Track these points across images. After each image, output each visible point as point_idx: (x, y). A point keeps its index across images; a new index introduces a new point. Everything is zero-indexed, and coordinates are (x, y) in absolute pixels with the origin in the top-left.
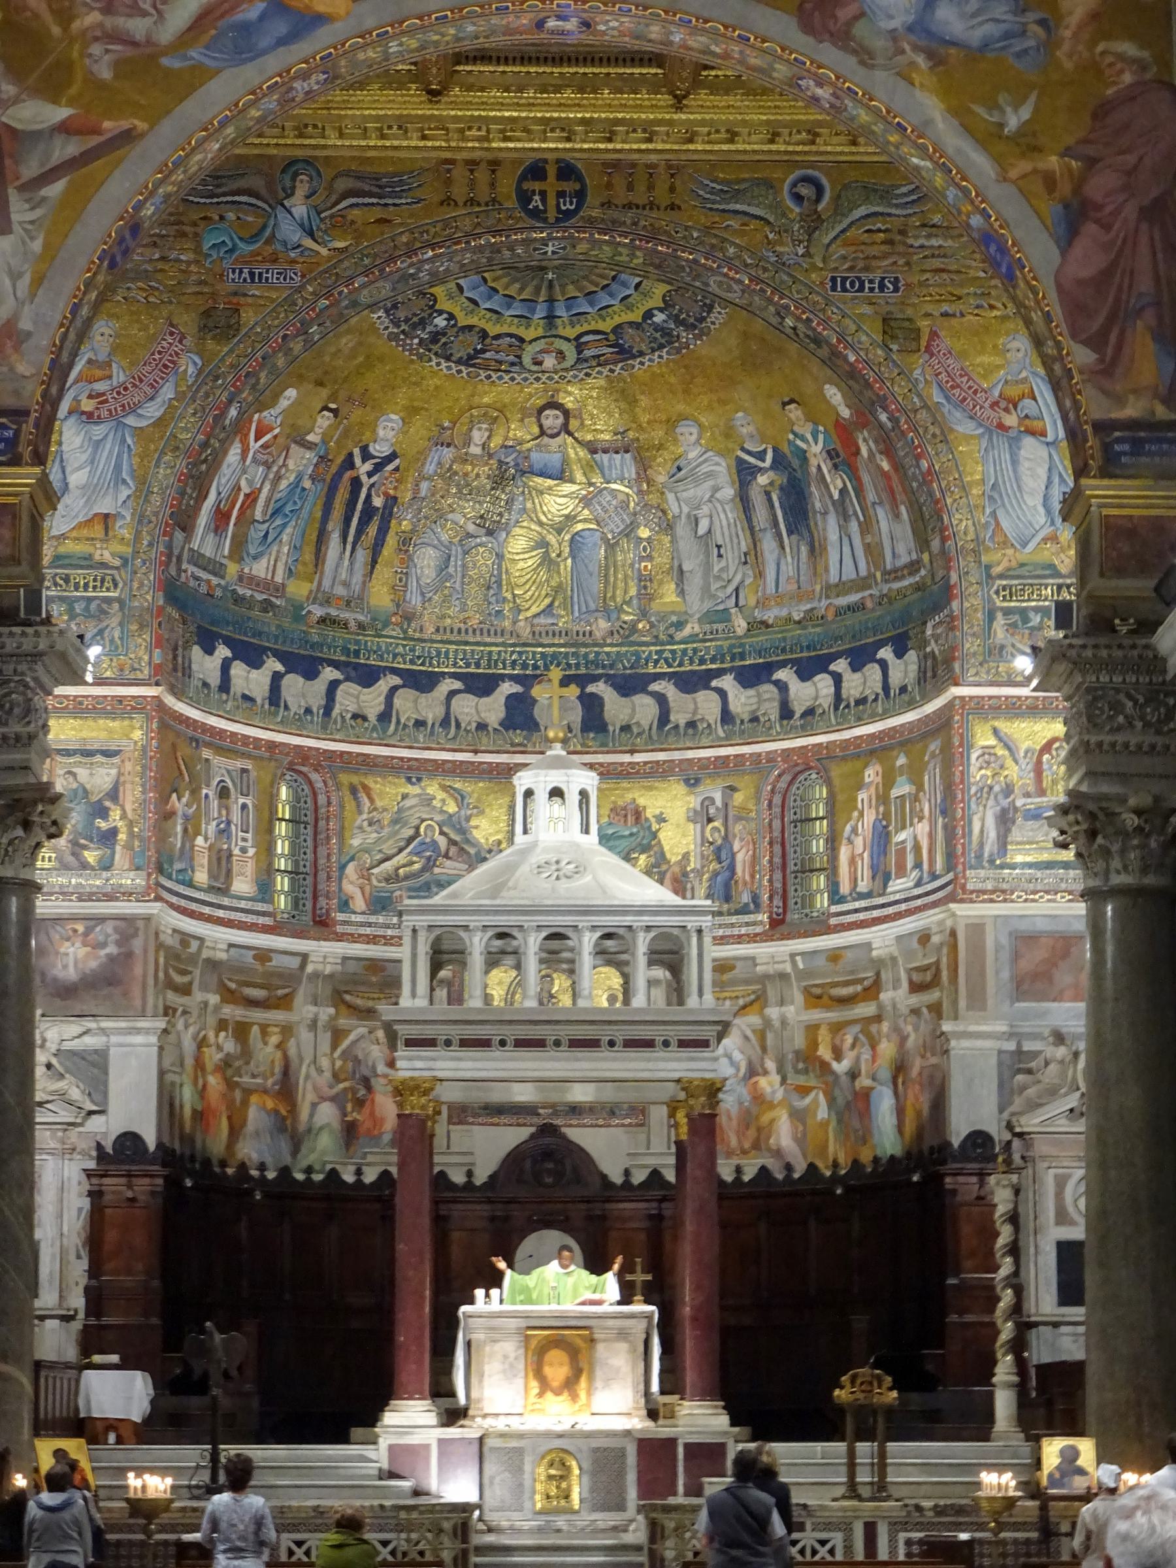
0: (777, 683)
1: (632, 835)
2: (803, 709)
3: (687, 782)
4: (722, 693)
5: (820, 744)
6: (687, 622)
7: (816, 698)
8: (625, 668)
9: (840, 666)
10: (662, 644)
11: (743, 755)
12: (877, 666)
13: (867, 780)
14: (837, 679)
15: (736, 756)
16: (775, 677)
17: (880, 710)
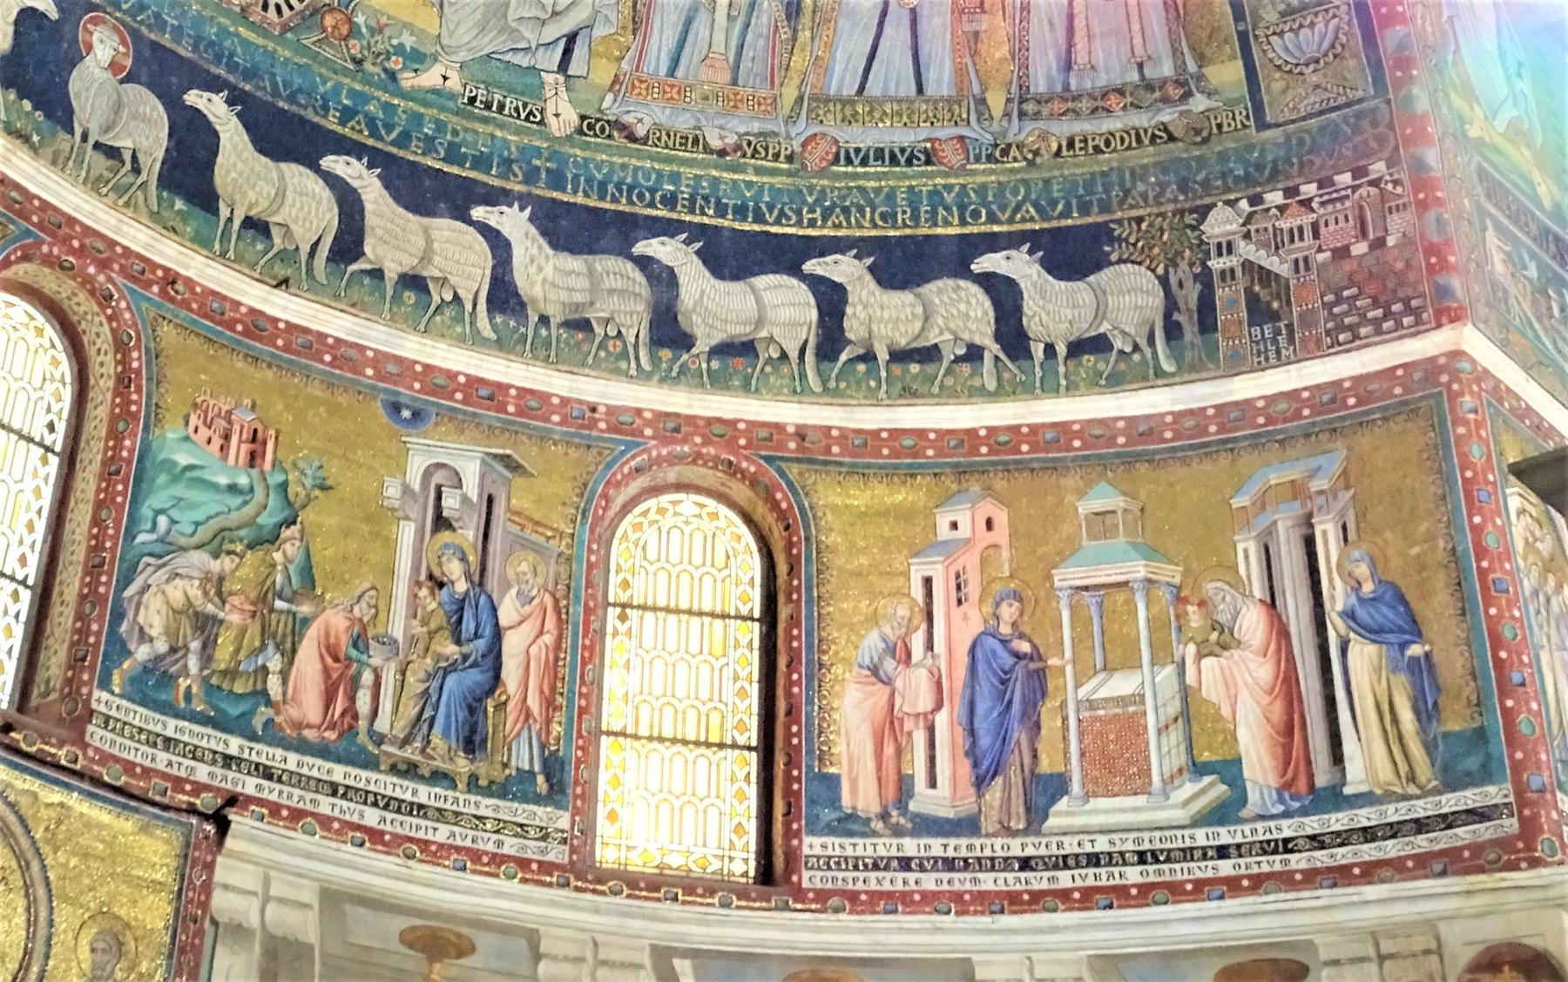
0: (644, 263)
1: (233, 488)
2: (717, 338)
3: (395, 408)
4: (498, 243)
5: (779, 427)
6: (436, 60)
7: (760, 322)
8: (276, 93)
9: (843, 269)
10: (367, 80)
11: (544, 397)
12: (975, 289)
13: (944, 532)
14: (831, 299)
15: (522, 391)
16: (640, 248)
17: (991, 385)
